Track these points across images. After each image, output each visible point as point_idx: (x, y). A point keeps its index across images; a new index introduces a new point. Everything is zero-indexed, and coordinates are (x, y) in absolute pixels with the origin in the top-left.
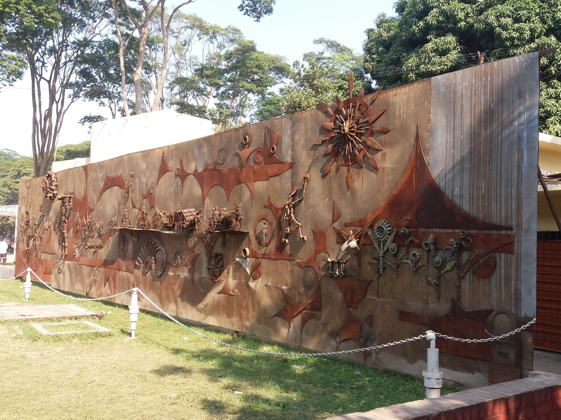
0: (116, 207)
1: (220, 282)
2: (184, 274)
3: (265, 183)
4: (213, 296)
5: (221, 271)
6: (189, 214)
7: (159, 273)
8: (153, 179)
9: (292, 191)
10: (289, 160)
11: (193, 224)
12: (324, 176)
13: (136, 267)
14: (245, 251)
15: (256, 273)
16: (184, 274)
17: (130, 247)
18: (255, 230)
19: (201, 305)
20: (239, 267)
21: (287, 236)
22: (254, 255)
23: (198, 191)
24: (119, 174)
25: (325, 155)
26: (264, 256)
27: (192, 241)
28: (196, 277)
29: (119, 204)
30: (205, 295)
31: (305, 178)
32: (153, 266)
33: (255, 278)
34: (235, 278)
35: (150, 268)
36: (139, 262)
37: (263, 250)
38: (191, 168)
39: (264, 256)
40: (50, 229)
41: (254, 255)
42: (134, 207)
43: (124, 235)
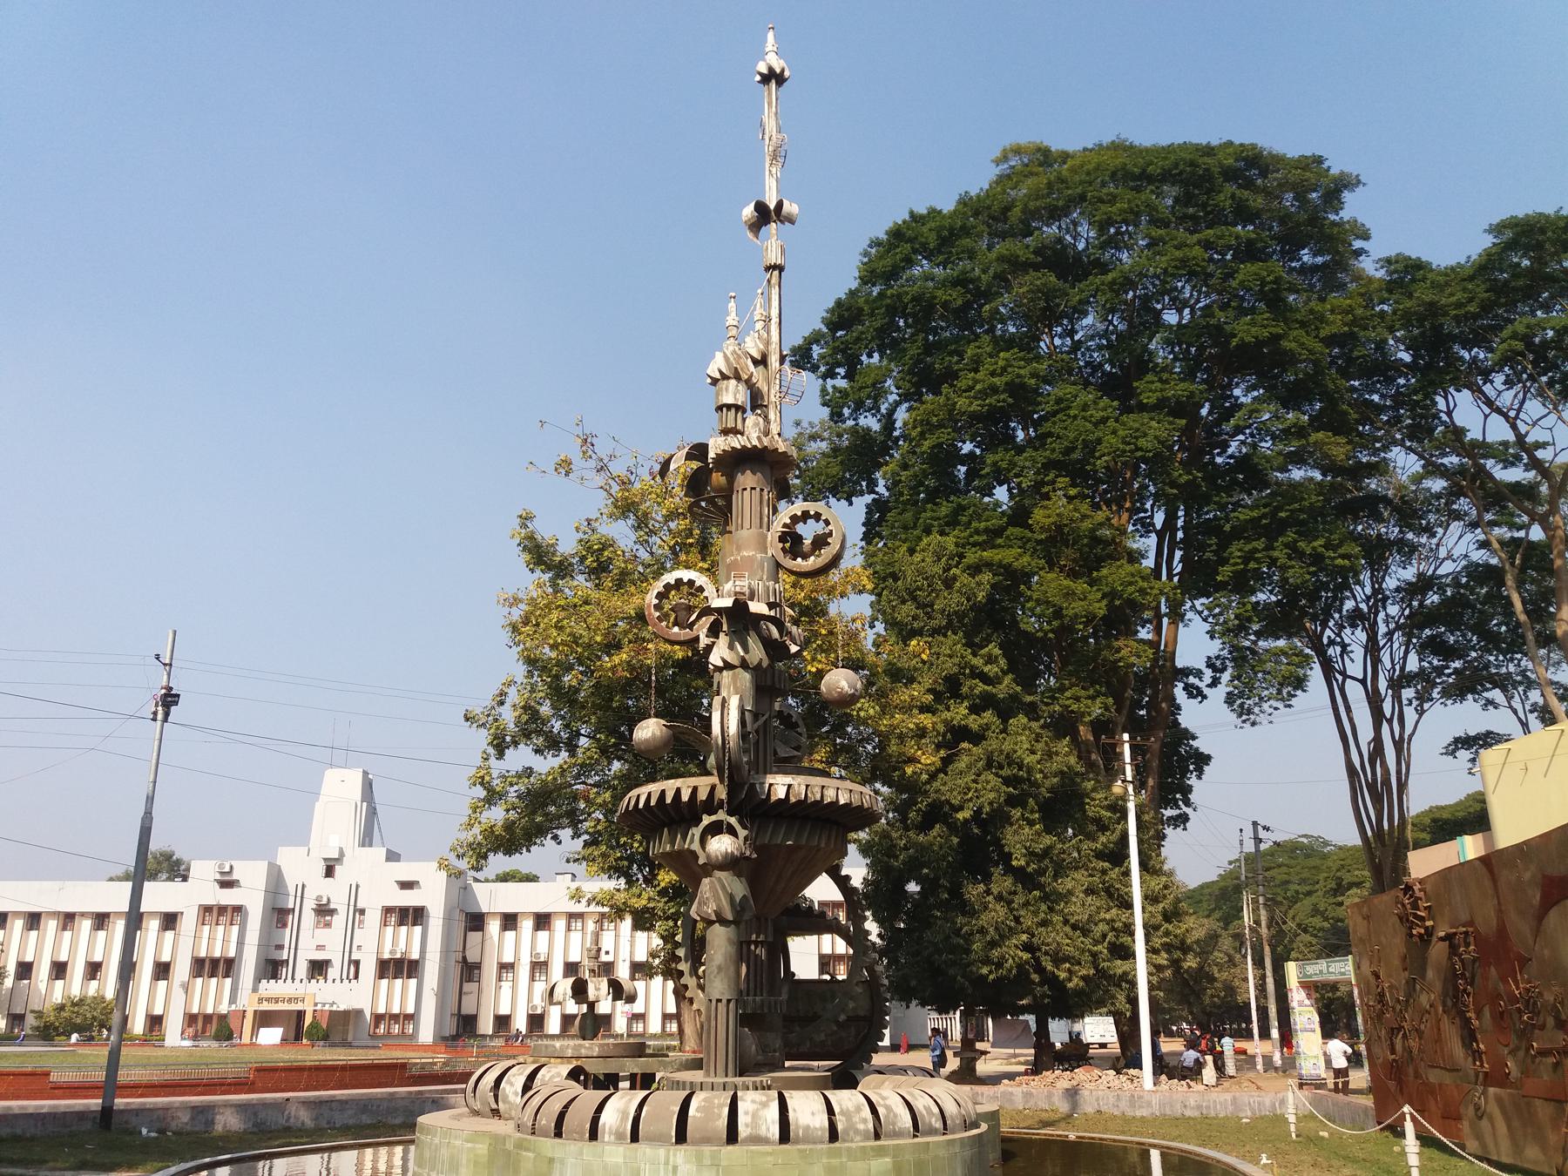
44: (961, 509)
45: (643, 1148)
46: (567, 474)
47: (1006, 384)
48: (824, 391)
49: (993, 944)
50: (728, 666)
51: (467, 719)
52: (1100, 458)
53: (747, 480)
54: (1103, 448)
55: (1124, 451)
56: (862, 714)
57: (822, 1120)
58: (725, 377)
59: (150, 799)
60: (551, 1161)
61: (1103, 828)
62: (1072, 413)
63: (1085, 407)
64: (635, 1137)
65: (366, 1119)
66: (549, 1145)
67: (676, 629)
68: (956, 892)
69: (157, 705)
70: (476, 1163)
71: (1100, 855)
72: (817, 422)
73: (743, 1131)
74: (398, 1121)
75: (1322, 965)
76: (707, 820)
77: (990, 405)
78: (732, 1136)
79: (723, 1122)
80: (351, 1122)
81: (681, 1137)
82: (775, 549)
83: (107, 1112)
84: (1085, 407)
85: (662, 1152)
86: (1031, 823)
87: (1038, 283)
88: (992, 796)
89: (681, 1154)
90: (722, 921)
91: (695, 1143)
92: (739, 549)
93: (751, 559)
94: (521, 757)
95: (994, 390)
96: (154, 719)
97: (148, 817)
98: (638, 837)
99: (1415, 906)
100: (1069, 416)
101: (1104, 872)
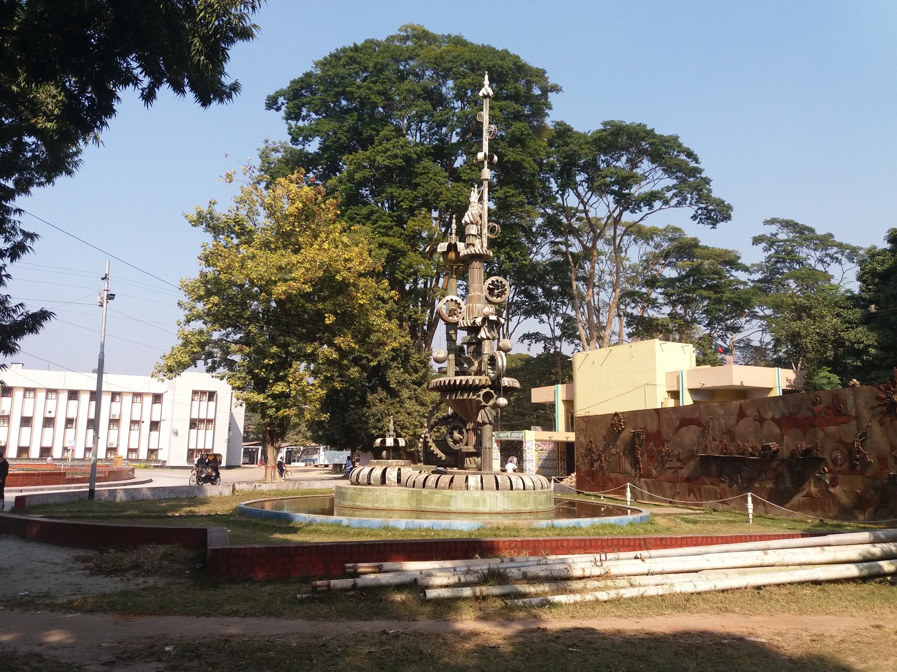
0: (695, 439)
1: (804, 490)
2: (770, 485)
3: (836, 428)
4: (798, 499)
5: (804, 483)
6: (773, 445)
7: (746, 486)
8: (732, 421)
9: (859, 433)
10: (854, 414)
11: (777, 451)
12: (881, 425)
13: (721, 481)
14: (824, 470)
15: (834, 483)
16: (770, 485)
17: (714, 468)
18: (830, 456)
19: (788, 505)
20: (819, 481)
21: (857, 460)
22: (830, 471)
23: (776, 430)
24: (696, 416)
25: (881, 413)
26: (840, 472)
27: (774, 465)
28: (781, 487)
29: (698, 438)
30: (791, 498)
31: (868, 426)
32: (740, 480)
33: (833, 486)
34: (816, 486)
35: (737, 482)
36: (725, 478)
37: (838, 469)
38: (770, 415)
39: (840, 472)
40: (619, 455)
41: (830, 471)
42: (714, 440)
43: (706, 461)
44: (372, 212)
45: (486, 493)
46: (230, 182)
47: (403, 154)
48: (290, 128)
49: (379, 421)
50: (488, 338)
51: (178, 303)
52: (441, 201)
53: (476, 264)
54: (443, 197)
55: (453, 201)
56: (375, 323)
57: (531, 484)
58: (472, 223)
59: (102, 346)
60: (450, 497)
61: (416, 371)
62: (430, 176)
63: (436, 175)
64: (482, 489)
65: (173, 496)
66: (448, 492)
67: (451, 318)
68: (363, 398)
69: (102, 298)
70: (401, 500)
71: (414, 383)
72: (277, 142)
73: (514, 487)
74: (185, 496)
75: (508, 433)
76: (484, 391)
77: (394, 164)
78: (512, 488)
79: (509, 484)
80: (167, 497)
81: (497, 488)
82: (486, 293)
83: (92, 492)
84: (436, 175)
85: (493, 493)
86: (399, 369)
87: (424, 107)
88: (386, 356)
89: (498, 493)
90: (490, 423)
91: (502, 490)
92: (474, 291)
93: (479, 296)
94: (198, 325)
95: (396, 156)
96: (102, 305)
97: (102, 353)
98: (264, 370)
99: (619, 421)
100: (428, 177)
101: (415, 390)
